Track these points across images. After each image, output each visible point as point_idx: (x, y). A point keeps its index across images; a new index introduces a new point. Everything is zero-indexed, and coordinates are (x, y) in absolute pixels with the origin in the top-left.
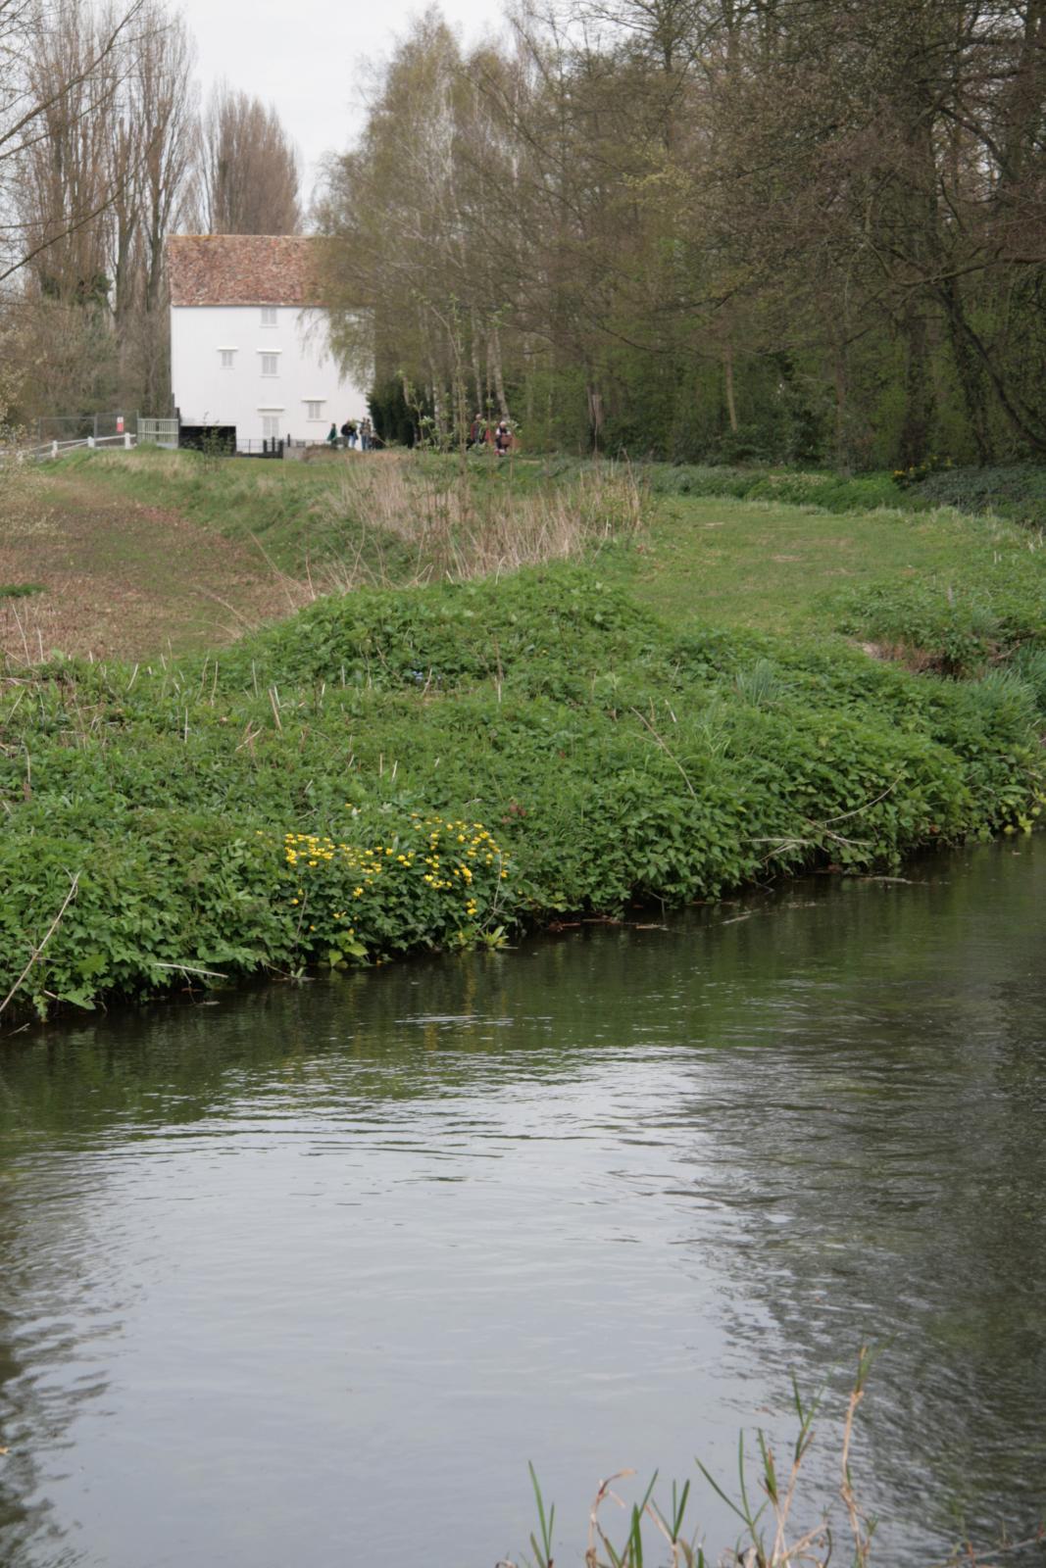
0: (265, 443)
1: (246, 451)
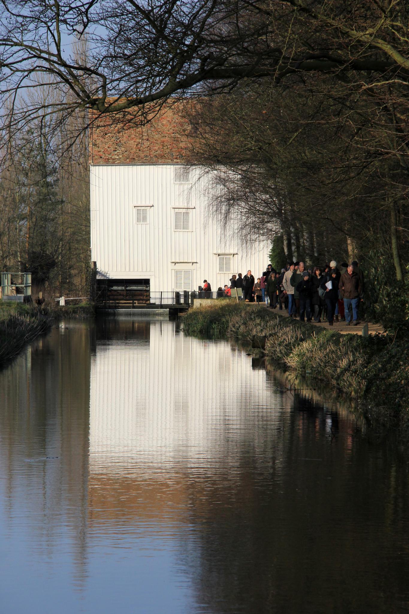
0: (178, 295)
1: (158, 302)
